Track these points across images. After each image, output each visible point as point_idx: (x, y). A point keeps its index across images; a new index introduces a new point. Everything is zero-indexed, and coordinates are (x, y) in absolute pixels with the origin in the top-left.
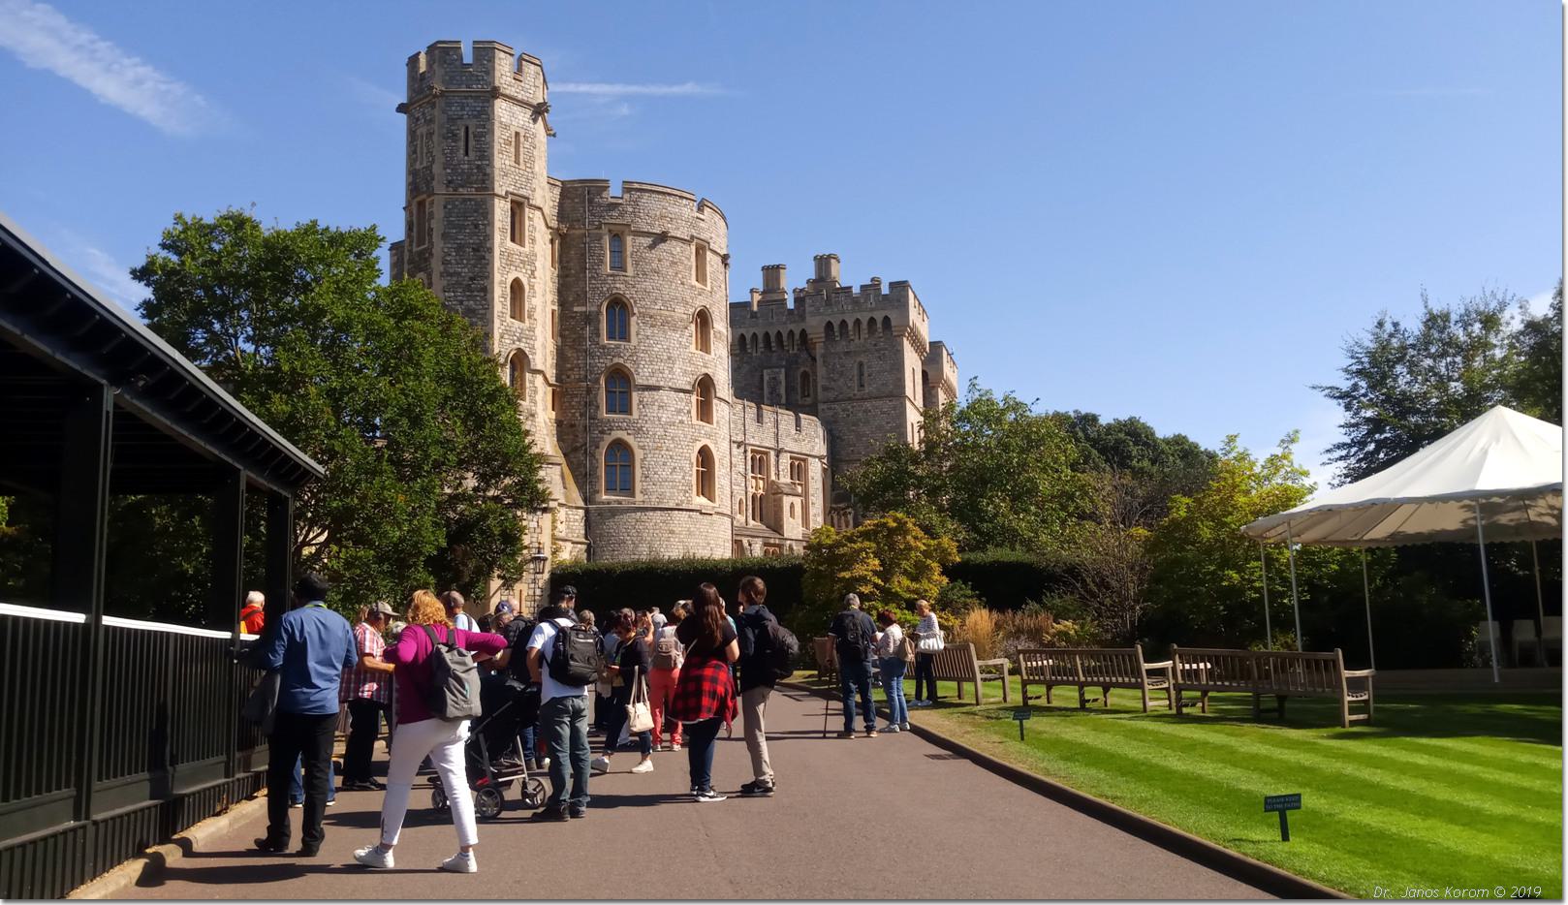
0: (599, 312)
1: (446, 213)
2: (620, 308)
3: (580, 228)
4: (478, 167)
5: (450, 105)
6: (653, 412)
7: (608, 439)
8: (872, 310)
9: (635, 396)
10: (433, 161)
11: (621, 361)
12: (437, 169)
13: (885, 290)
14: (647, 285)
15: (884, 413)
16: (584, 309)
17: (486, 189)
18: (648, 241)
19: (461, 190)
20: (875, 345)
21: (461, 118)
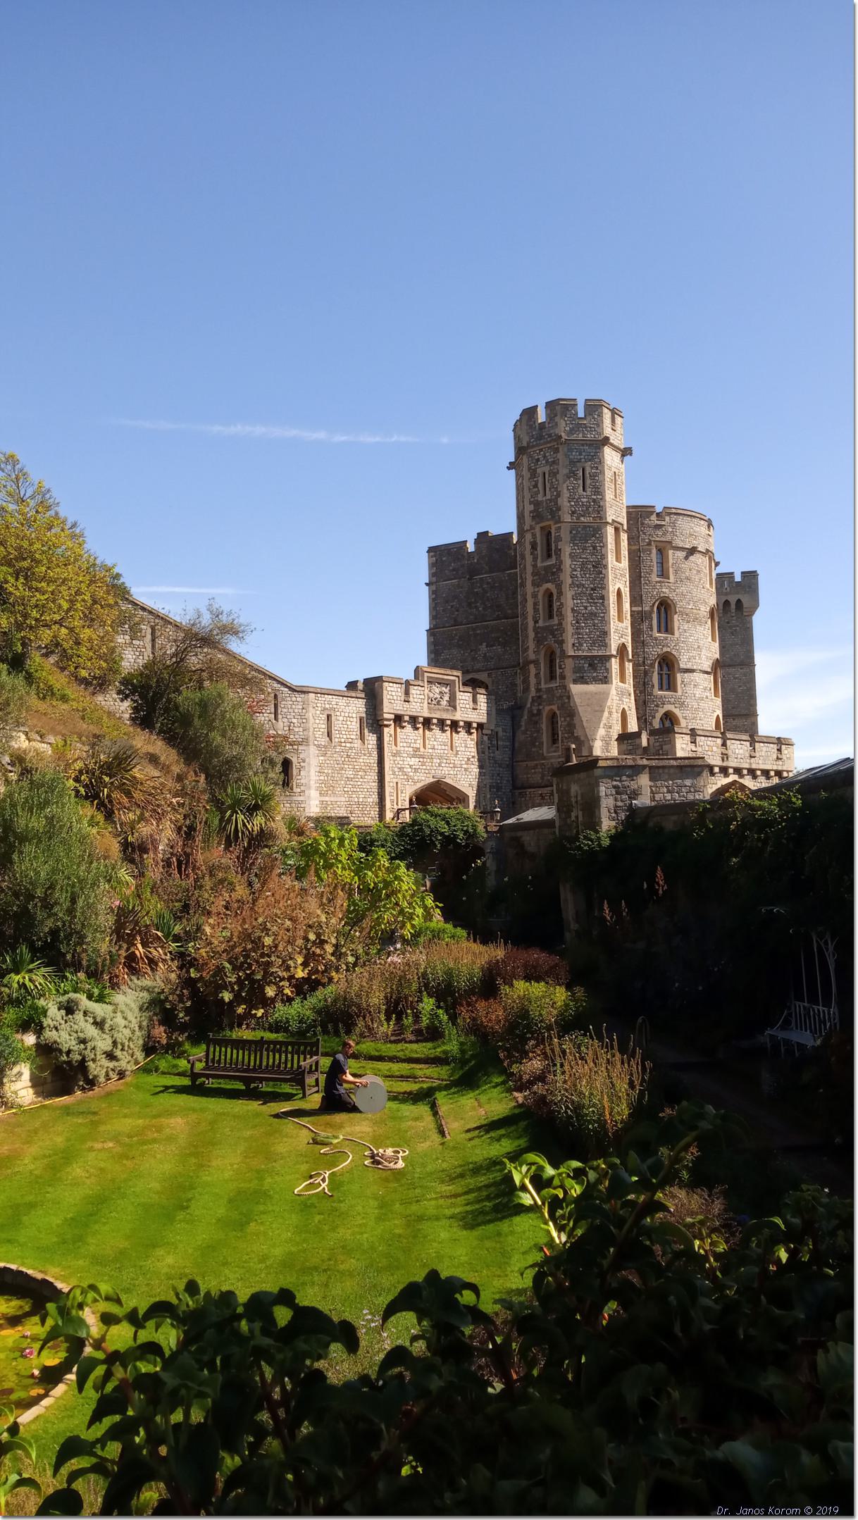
0: (651, 612)
1: (572, 537)
2: (666, 607)
3: (635, 545)
4: (594, 501)
5: (570, 450)
6: (689, 690)
7: (661, 711)
8: (726, 594)
9: (679, 676)
10: (559, 495)
11: (669, 650)
12: (564, 502)
13: (738, 578)
14: (683, 589)
15: (735, 678)
16: (640, 609)
17: (601, 518)
18: (682, 554)
19: (582, 519)
20: (728, 623)
21: (579, 461)
